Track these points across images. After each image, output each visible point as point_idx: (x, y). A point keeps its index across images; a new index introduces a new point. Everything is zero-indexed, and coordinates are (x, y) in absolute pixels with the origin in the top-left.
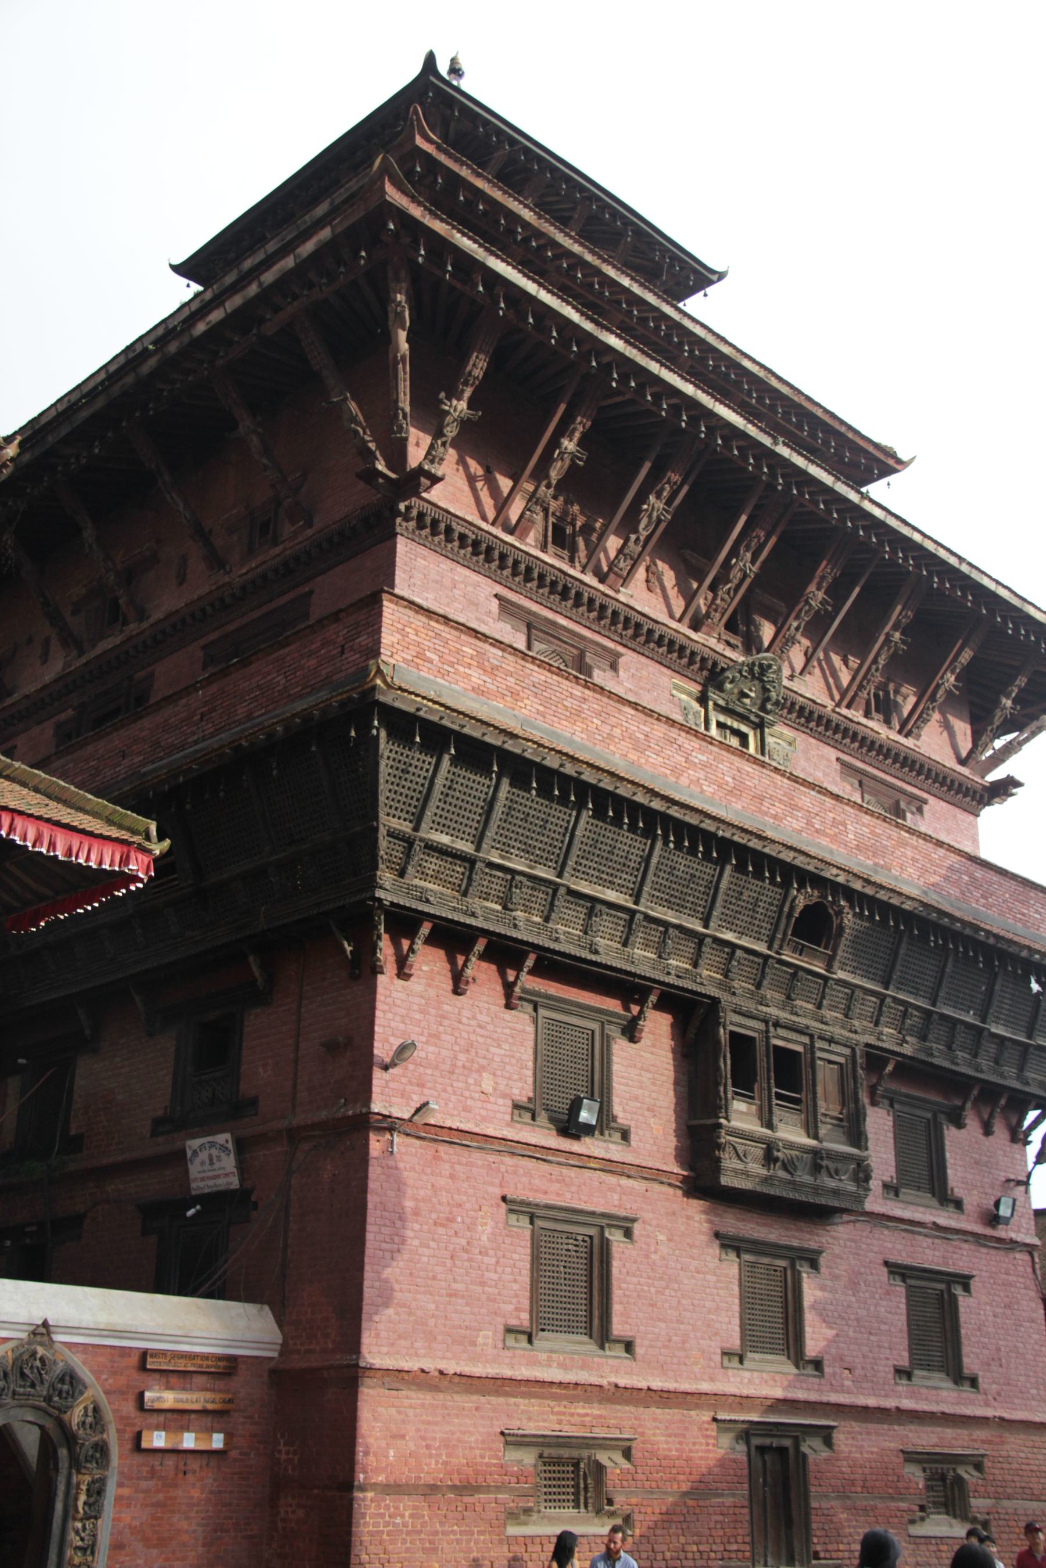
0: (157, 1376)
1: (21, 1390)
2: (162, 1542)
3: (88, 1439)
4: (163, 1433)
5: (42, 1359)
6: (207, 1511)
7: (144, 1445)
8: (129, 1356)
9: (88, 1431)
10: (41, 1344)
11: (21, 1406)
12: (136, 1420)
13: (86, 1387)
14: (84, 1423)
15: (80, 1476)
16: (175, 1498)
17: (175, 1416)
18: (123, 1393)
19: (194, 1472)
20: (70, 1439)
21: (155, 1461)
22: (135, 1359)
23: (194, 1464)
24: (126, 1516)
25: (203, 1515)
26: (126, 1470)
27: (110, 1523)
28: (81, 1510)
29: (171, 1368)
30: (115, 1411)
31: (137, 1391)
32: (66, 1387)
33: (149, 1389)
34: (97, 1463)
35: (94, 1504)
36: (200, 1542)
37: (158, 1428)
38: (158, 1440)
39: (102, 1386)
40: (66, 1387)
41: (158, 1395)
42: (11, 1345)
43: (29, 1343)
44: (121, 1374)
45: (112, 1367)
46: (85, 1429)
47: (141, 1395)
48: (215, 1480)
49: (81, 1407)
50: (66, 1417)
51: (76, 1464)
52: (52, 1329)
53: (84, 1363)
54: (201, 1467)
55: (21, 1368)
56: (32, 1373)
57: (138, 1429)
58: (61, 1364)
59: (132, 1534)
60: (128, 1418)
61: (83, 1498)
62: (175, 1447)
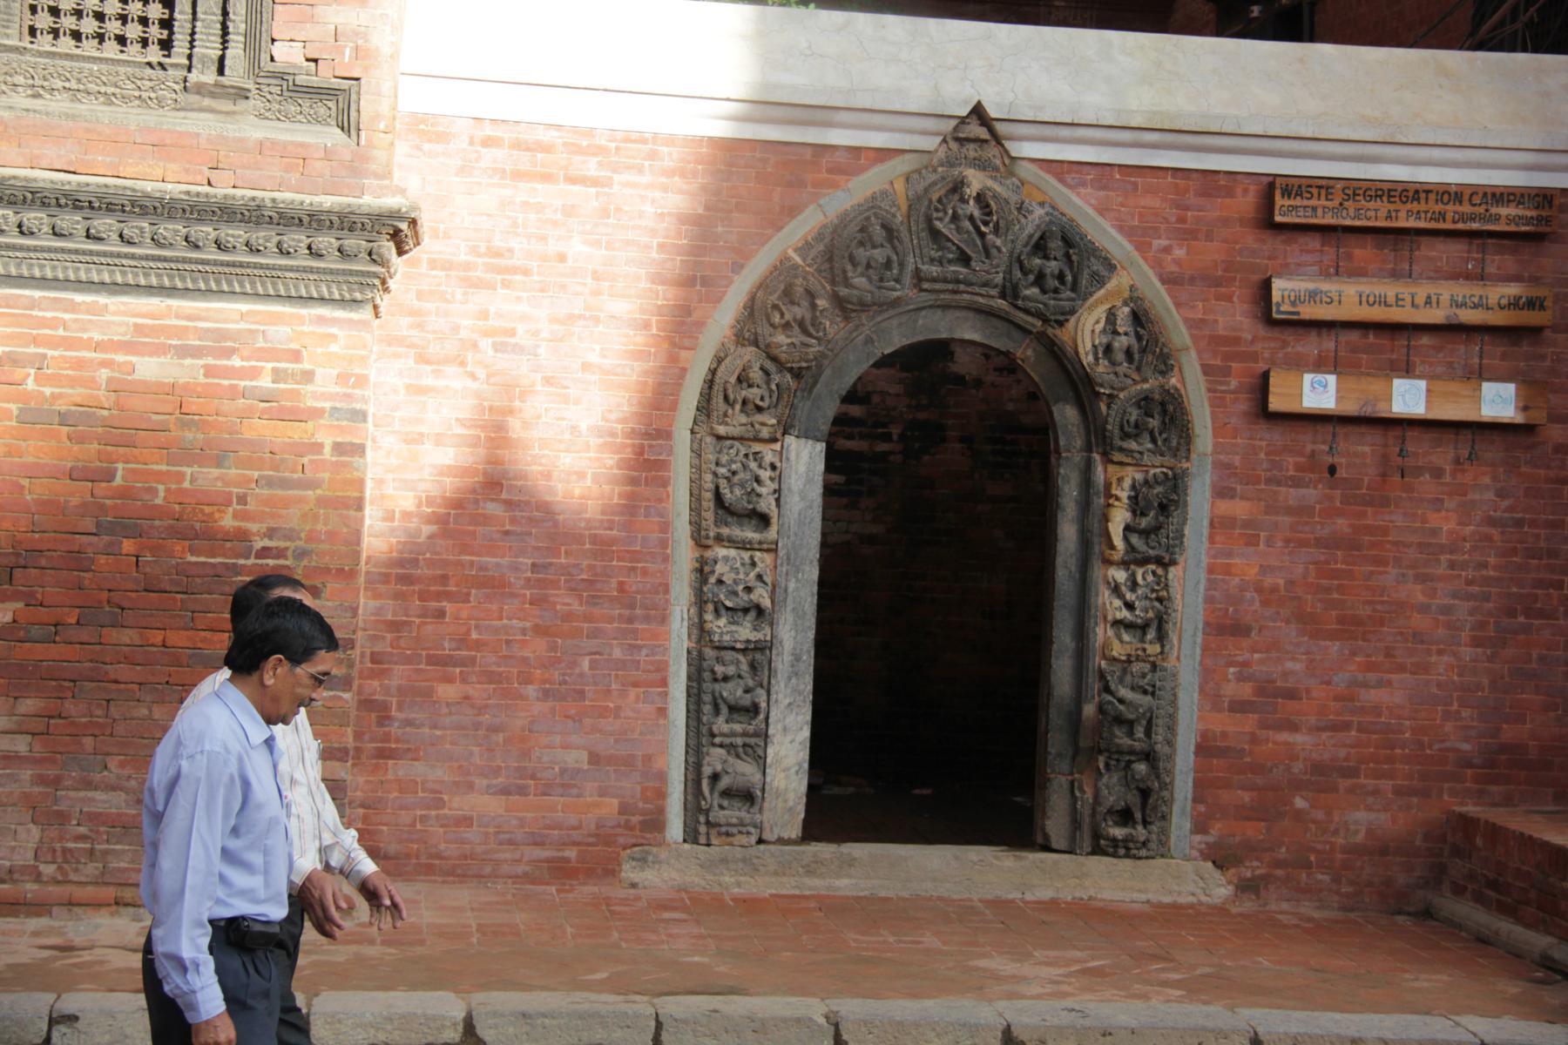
0: (1313, 242)
1: (935, 270)
2: (1351, 628)
3: (1125, 388)
4: (1332, 379)
5: (980, 198)
6: (1485, 565)
7: (1275, 404)
8: (1230, 193)
9: (1124, 367)
10: (982, 165)
11: (946, 307)
12: (1258, 347)
13: (1112, 268)
14: (1108, 349)
15: (1111, 468)
16: (1385, 531)
17: (1383, 341)
18: (1217, 283)
19: (1437, 473)
20: (1081, 386)
21: (1312, 442)
22: (1246, 202)
23: (1442, 455)
24: (1247, 564)
25: (1470, 573)
26: (1237, 460)
27: (1203, 576)
28: (1118, 541)
29: (1348, 222)
30: (1192, 324)
31: (1257, 277)
32: (1053, 266)
33: (1286, 271)
34: (1154, 441)
35: (1157, 529)
36: (1465, 635)
37: (1320, 366)
38: (1319, 393)
39: (1157, 264)
40: (1053, 266)
41: (1311, 286)
42: (900, 166)
43: (950, 163)
44: (1209, 237)
45: (1182, 220)
46: (1113, 363)
47: (1266, 286)
48: (1501, 494)
49: (1100, 312)
50: (1063, 335)
51: (1099, 439)
52: (999, 127)
53: (1101, 211)
54: (1457, 461)
55: (929, 220)
56: (959, 229)
57: (1262, 366)
58: (1039, 212)
59: (1265, 603)
60: (1237, 341)
61: (1119, 518)
62: (1368, 411)
